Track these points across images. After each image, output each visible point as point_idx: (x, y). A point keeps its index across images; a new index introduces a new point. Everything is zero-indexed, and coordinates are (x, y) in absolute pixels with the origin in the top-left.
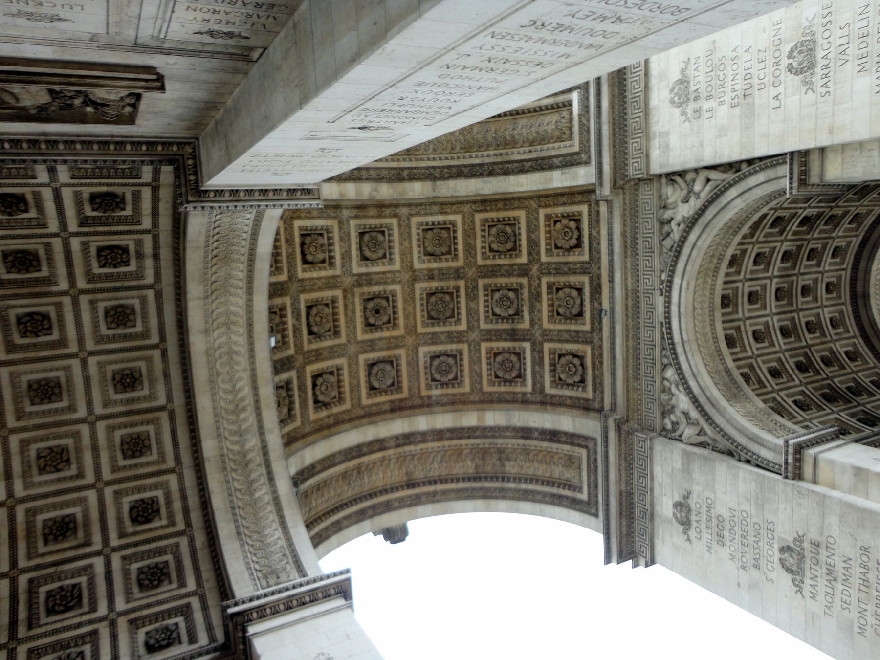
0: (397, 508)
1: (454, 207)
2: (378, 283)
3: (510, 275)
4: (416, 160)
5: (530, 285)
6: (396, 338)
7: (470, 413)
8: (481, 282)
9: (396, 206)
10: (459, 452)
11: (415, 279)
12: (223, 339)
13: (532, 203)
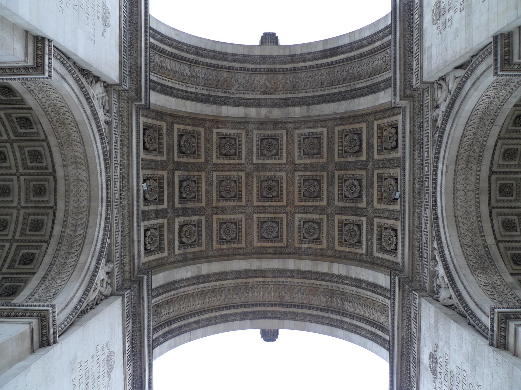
0: (270, 318)
1: (323, 123)
2: (270, 171)
3: (356, 169)
5: (367, 175)
6: (281, 207)
8: (337, 174)
9: (286, 123)
10: (316, 289)
11: (295, 170)
12: (75, 171)
13: (370, 117)
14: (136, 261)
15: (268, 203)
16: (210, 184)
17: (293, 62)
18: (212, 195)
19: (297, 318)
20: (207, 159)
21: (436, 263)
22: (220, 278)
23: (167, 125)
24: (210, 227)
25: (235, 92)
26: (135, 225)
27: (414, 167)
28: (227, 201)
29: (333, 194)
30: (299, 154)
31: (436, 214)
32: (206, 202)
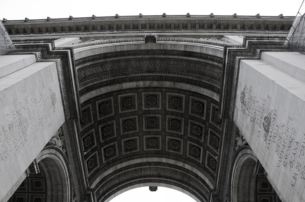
0: (153, 182)
1: (183, 92)
2: (152, 114)
3: (199, 122)
6: (159, 132)
7: (180, 162)
8: (190, 121)
15: (151, 130)
16: (118, 125)
17: (165, 54)
18: (120, 130)
27: (225, 150)
29: (187, 130)
31: (230, 182)
32: (117, 134)
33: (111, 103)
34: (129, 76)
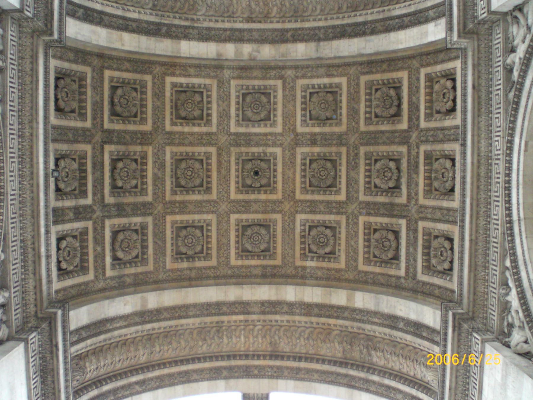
0: (256, 376)
1: (340, 70)
2: (257, 145)
3: (392, 143)
4: (302, 21)
5: (409, 152)
6: (274, 202)
8: (362, 150)
9: (283, 68)
13: (414, 62)
14: (44, 288)
15: (252, 197)
16: (160, 165)
18: (163, 181)
19: (298, 376)
20: (156, 126)
21: (508, 290)
22: (177, 315)
23: (93, 71)
24: (161, 235)
25: (201, 19)
26: (43, 230)
27: (479, 142)
28: (188, 192)
29: (357, 182)
30: (303, 118)
32: (154, 194)
33: (145, 93)
34: (199, 25)
